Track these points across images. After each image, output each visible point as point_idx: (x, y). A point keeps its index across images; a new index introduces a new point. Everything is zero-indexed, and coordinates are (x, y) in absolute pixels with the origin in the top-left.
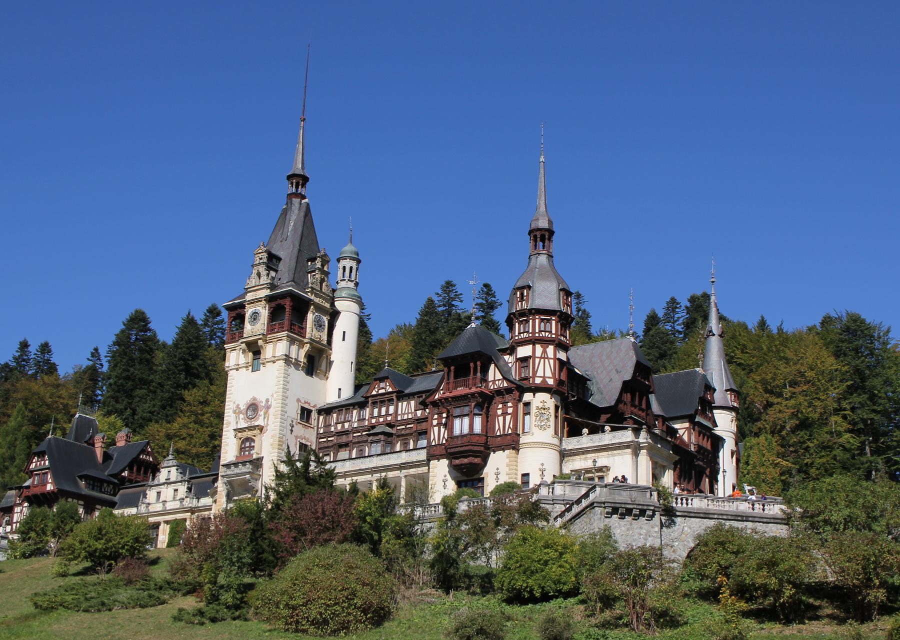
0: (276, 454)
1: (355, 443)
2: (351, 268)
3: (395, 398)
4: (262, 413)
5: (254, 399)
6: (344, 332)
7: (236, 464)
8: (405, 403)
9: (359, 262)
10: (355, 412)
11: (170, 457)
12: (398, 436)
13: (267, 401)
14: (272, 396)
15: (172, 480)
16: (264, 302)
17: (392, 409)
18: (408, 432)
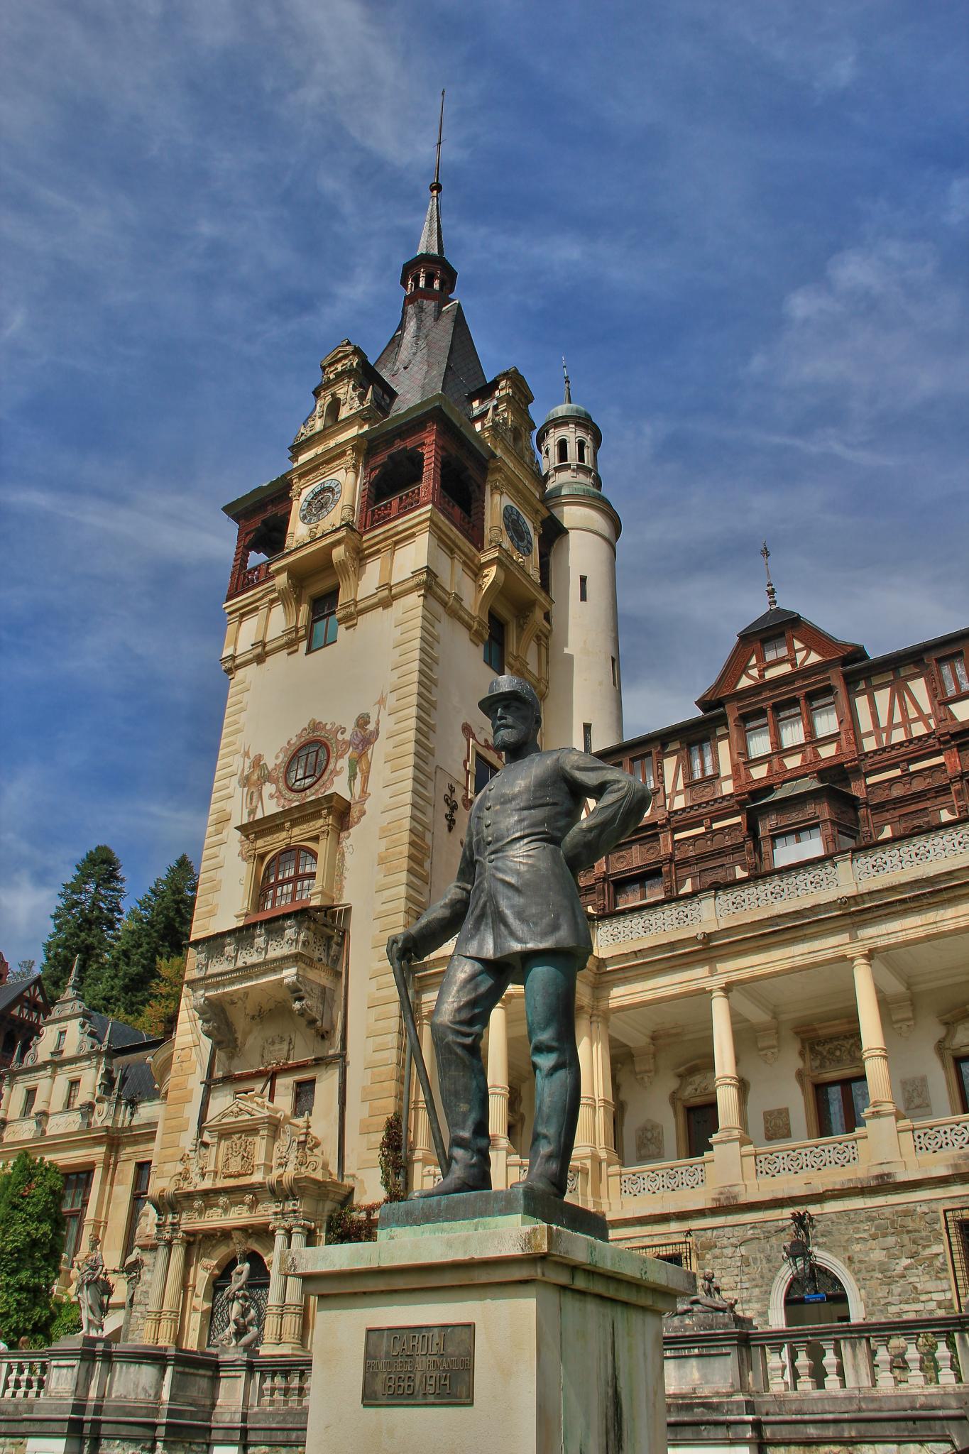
0: (402, 890)
1: (685, 863)
2: (581, 445)
3: (837, 681)
4: (344, 763)
5: (315, 726)
6: (583, 580)
7: (243, 935)
8: (883, 697)
9: (597, 440)
10: (670, 764)
11: (70, 993)
12: (880, 807)
13: (363, 721)
14: (381, 702)
15: (66, 1055)
16: (349, 458)
17: (827, 724)
18: (918, 785)
